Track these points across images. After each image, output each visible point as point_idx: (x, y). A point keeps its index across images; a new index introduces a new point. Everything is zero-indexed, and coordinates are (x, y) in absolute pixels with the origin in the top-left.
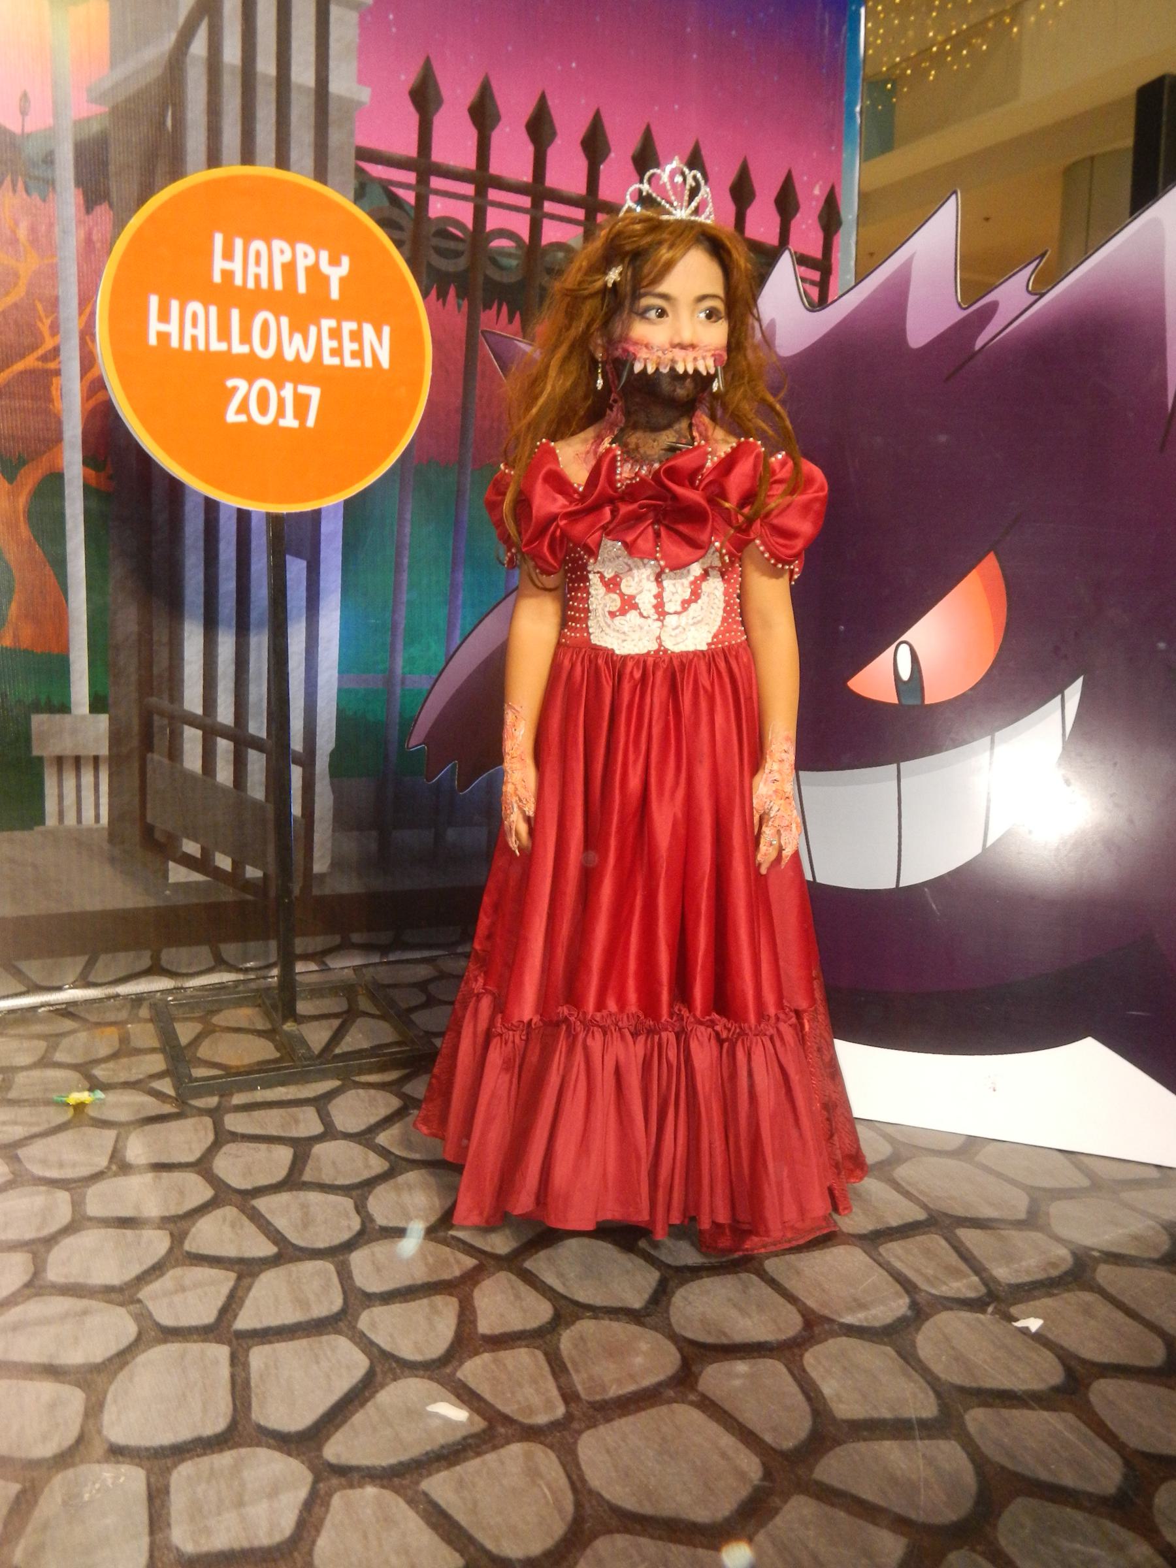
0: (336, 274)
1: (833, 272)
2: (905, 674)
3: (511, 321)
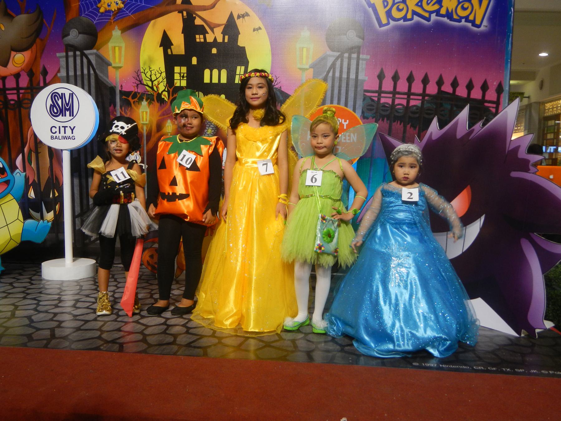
0: (345, 124)
1: (501, 103)
3: (400, 124)
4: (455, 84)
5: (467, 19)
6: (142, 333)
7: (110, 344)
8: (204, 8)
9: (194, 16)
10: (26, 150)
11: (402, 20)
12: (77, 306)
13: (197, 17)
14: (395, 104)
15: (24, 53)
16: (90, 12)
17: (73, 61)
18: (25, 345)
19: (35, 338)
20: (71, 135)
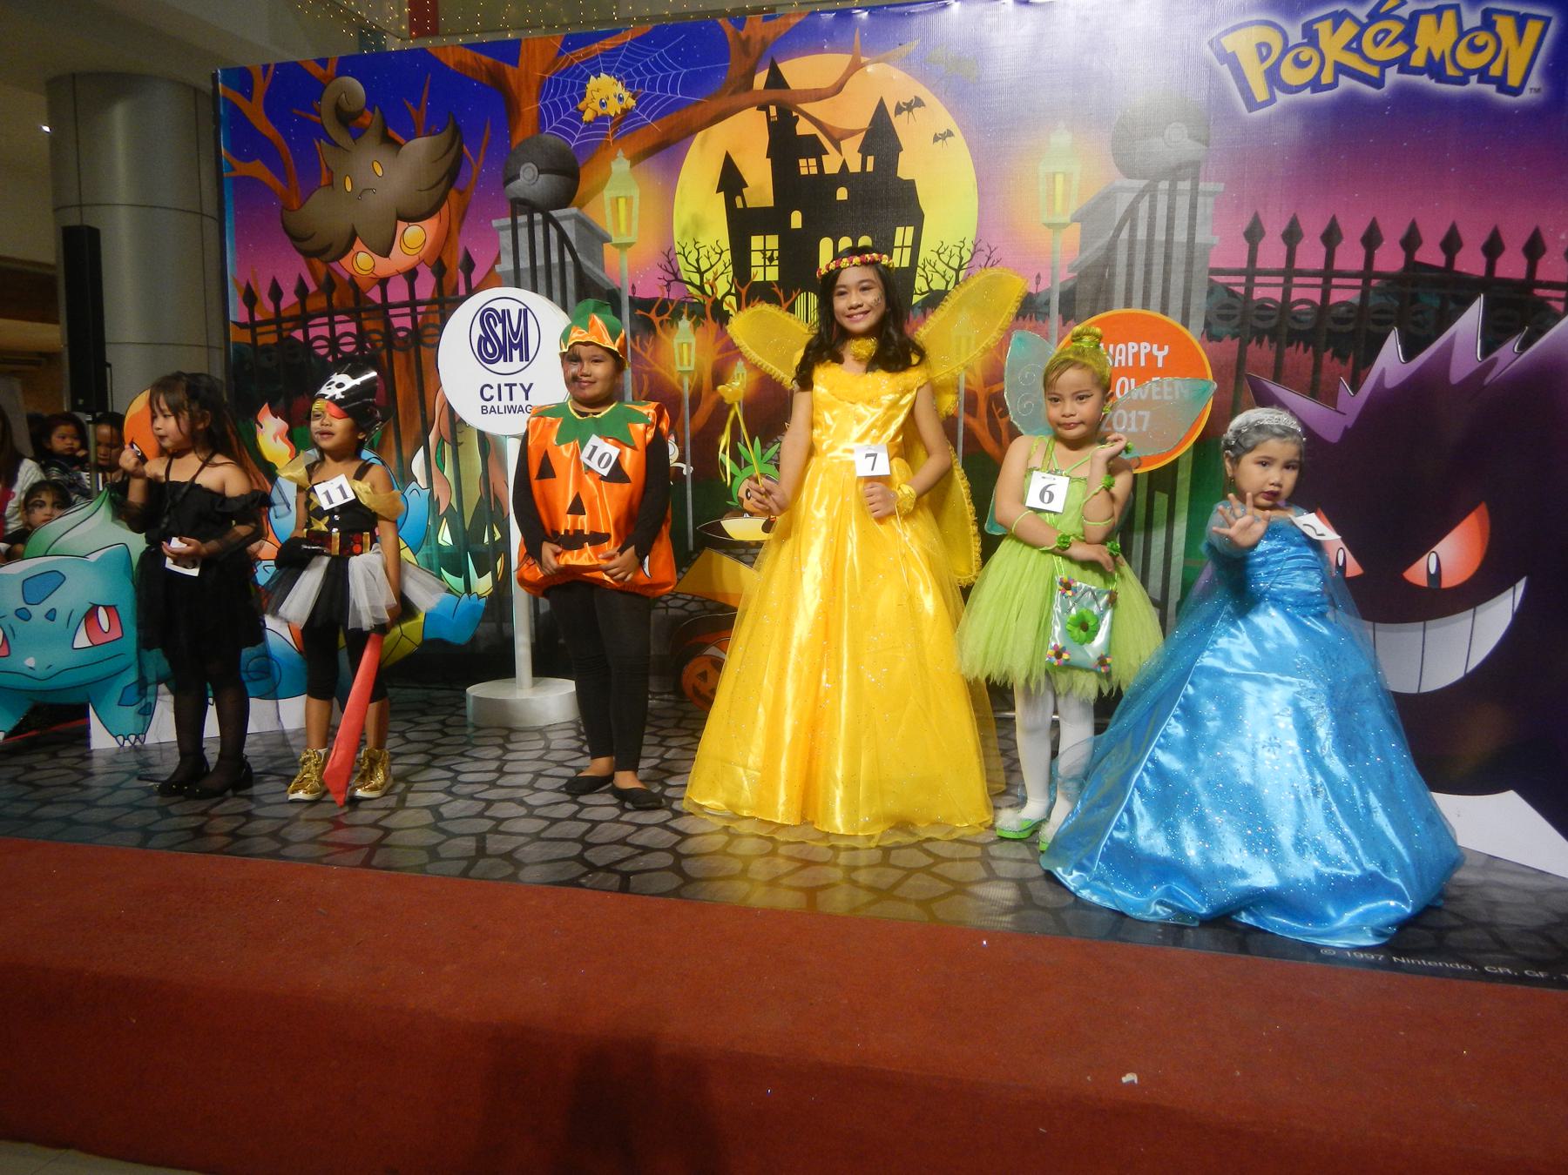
0: (1160, 355)
2: (1433, 570)
3: (1306, 350)
4: (1451, 244)
5: (1483, 74)
6: (672, 850)
7: (601, 874)
8: (818, 95)
9: (794, 114)
10: (432, 437)
11: (1309, 89)
12: (536, 786)
13: (802, 120)
14: (1292, 299)
15: (424, 223)
16: (564, 122)
17: (527, 236)
18: (421, 868)
19: (443, 855)
20: (524, 404)
